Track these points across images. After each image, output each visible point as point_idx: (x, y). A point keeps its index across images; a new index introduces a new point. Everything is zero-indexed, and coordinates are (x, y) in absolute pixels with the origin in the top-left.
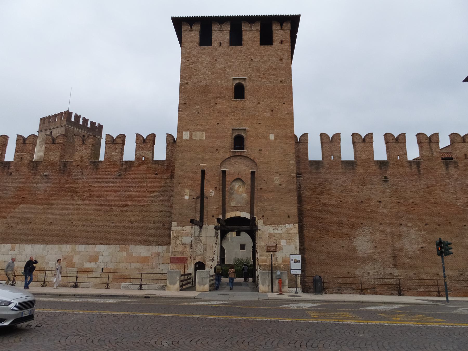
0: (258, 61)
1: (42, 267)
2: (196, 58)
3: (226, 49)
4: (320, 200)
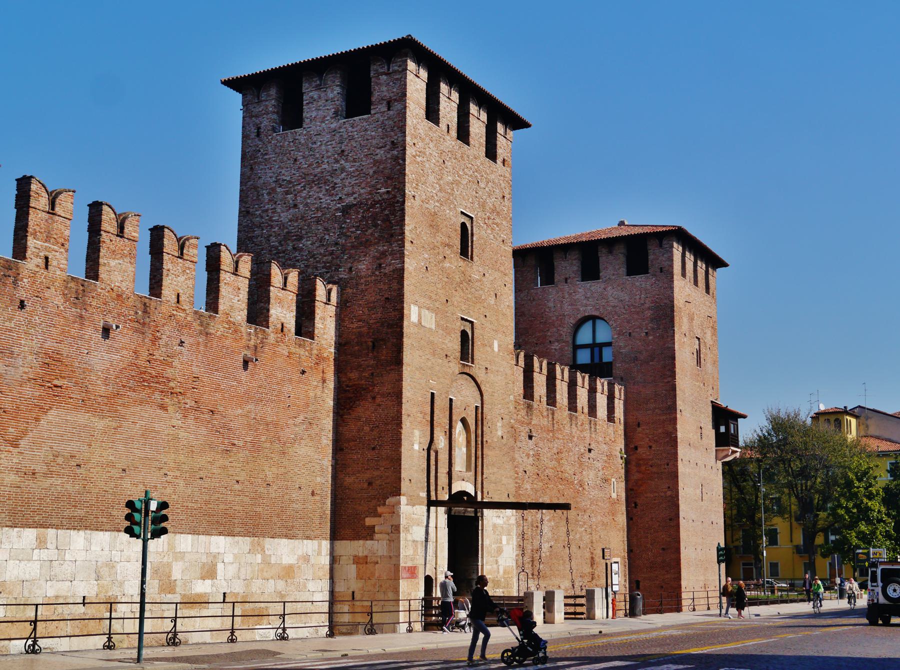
1: (110, 594)
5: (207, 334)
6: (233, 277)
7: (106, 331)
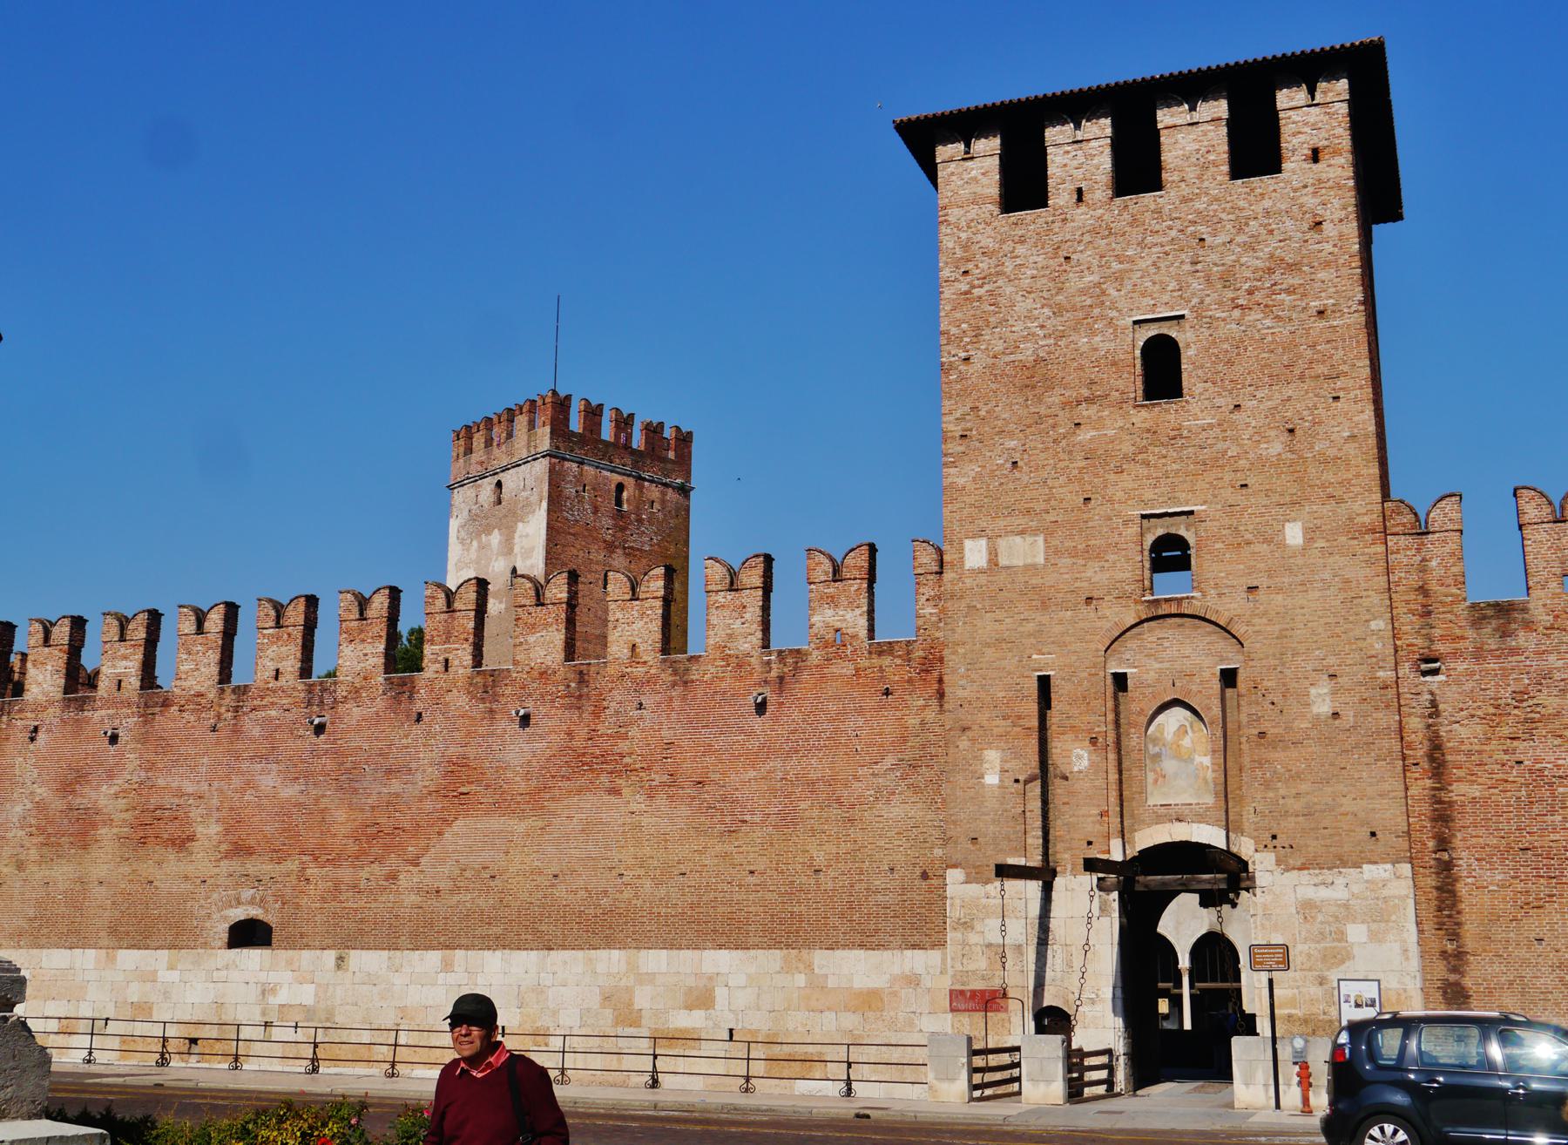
0: (1224, 244)
2: (993, 262)
3: (1101, 211)
4: (1522, 757)
5: (686, 683)
6: (730, 595)
7: (525, 720)
